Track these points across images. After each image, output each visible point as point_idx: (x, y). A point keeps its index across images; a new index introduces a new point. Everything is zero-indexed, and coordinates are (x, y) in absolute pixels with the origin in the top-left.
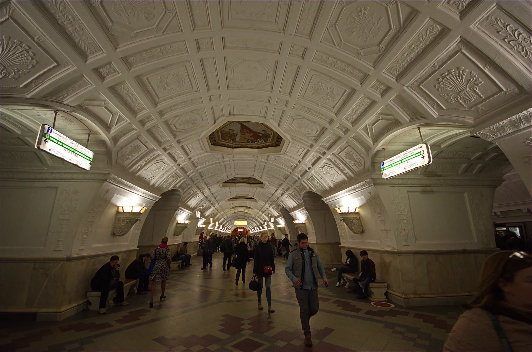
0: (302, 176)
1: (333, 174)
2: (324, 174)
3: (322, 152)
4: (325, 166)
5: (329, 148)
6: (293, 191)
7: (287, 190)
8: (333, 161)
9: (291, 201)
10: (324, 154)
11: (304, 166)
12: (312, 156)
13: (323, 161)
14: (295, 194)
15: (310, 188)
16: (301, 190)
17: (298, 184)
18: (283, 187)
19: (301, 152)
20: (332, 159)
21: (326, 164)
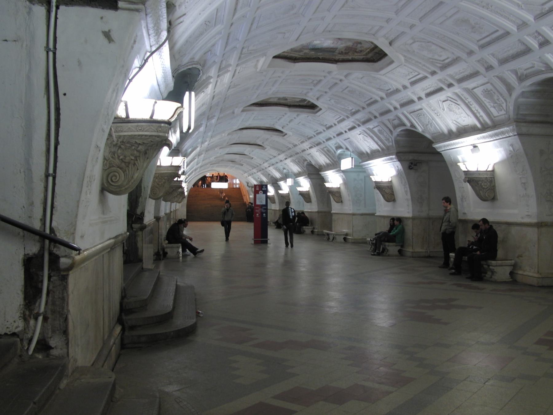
0: (403, 105)
1: (459, 113)
2: (444, 109)
3: (448, 83)
4: (447, 100)
5: (460, 81)
6: (376, 124)
7: (364, 123)
8: (463, 97)
9: (370, 140)
10: (450, 85)
11: (410, 94)
12: (431, 83)
13: (448, 93)
14: (379, 131)
15: (412, 125)
16: (395, 127)
17: (391, 116)
18: (359, 116)
19: (411, 76)
20: (462, 95)
21: (449, 99)
